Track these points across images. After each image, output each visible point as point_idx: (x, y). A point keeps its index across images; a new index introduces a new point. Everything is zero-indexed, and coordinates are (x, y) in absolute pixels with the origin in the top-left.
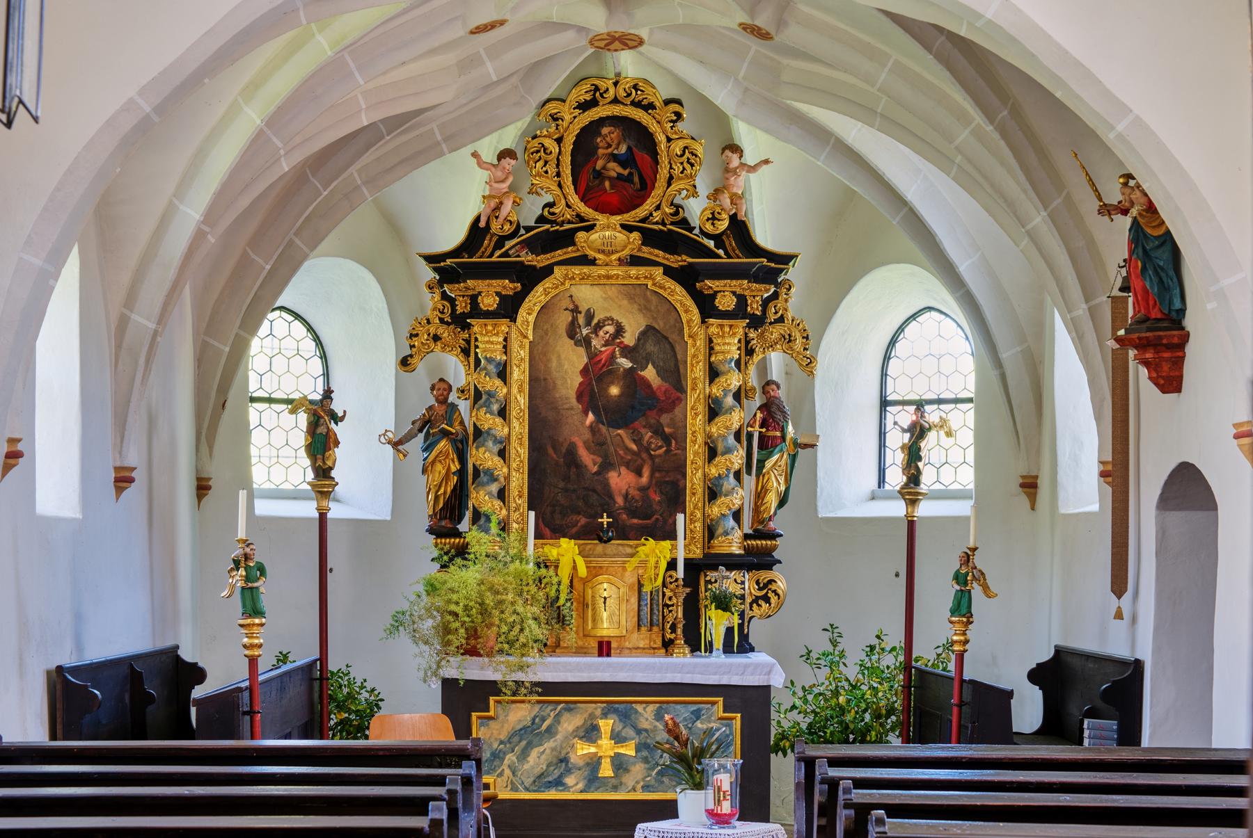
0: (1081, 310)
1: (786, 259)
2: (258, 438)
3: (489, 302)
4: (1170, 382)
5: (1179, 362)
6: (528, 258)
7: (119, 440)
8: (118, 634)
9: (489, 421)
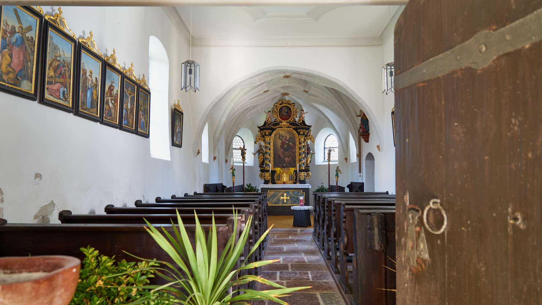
0: (354, 132)
1: (310, 126)
2: (234, 154)
3: (267, 133)
4: (367, 141)
5: (368, 138)
6: (273, 127)
7: (238, 235)
8: (214, 180)
9: (268, 151)
